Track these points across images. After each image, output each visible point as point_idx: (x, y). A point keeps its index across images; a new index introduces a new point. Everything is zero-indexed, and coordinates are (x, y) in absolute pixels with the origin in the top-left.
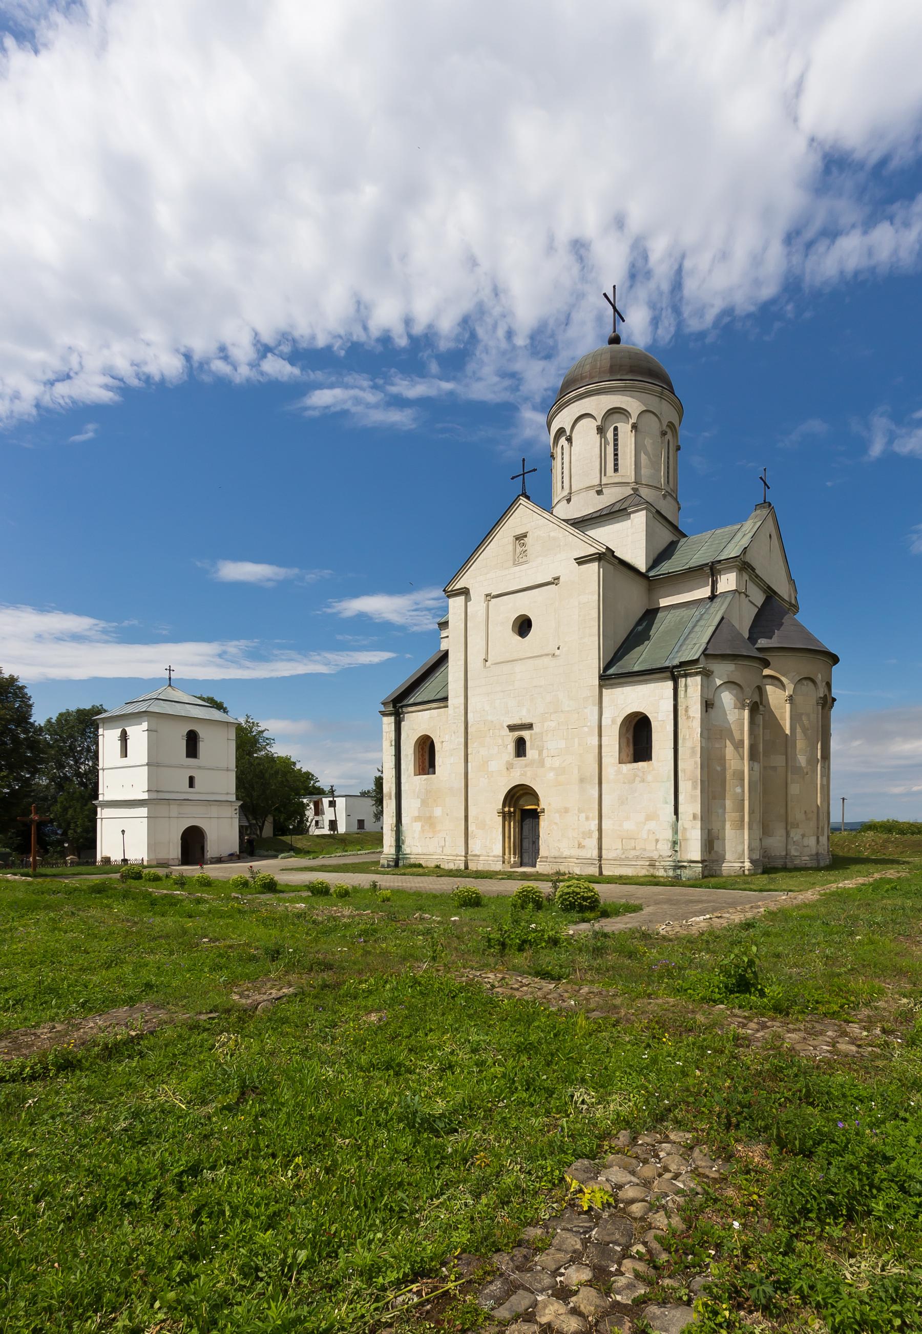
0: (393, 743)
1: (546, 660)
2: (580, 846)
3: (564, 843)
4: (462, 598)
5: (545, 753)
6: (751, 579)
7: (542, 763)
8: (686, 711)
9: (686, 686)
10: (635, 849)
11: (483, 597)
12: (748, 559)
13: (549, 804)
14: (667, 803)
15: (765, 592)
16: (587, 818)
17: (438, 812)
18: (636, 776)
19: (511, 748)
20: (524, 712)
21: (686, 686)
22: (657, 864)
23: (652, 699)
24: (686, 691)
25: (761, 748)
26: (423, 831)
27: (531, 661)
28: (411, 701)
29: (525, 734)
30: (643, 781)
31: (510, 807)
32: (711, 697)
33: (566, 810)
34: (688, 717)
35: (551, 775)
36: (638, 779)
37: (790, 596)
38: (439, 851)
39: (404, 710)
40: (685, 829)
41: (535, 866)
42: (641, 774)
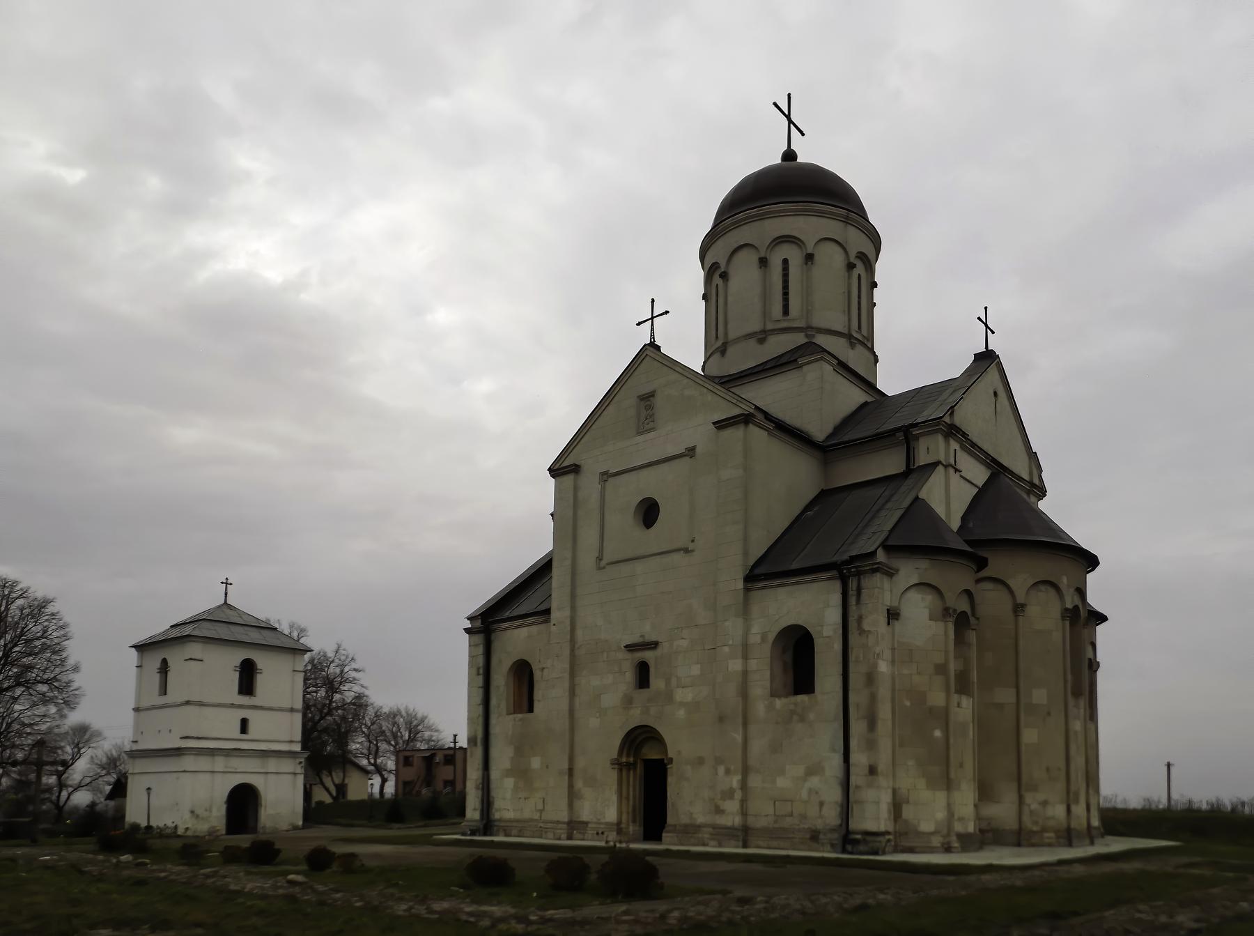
2: (719, 811)
5: (674, 681)
6: (963, 448)
7: (669, 697)
12: (957, 420)
13: (679, 752)
15: (988, 466)
16: (728, 772)
19: (630, 676)
20: (647, 628)
25: (974, 676)
28: (507, 614)
29: (648, 656)
30: (802, 719)
31: (628, 756)
32: (895, 604)
35: (681, 713)
36: (795, 718)
37: (1031, 474)
39: (496, 626)
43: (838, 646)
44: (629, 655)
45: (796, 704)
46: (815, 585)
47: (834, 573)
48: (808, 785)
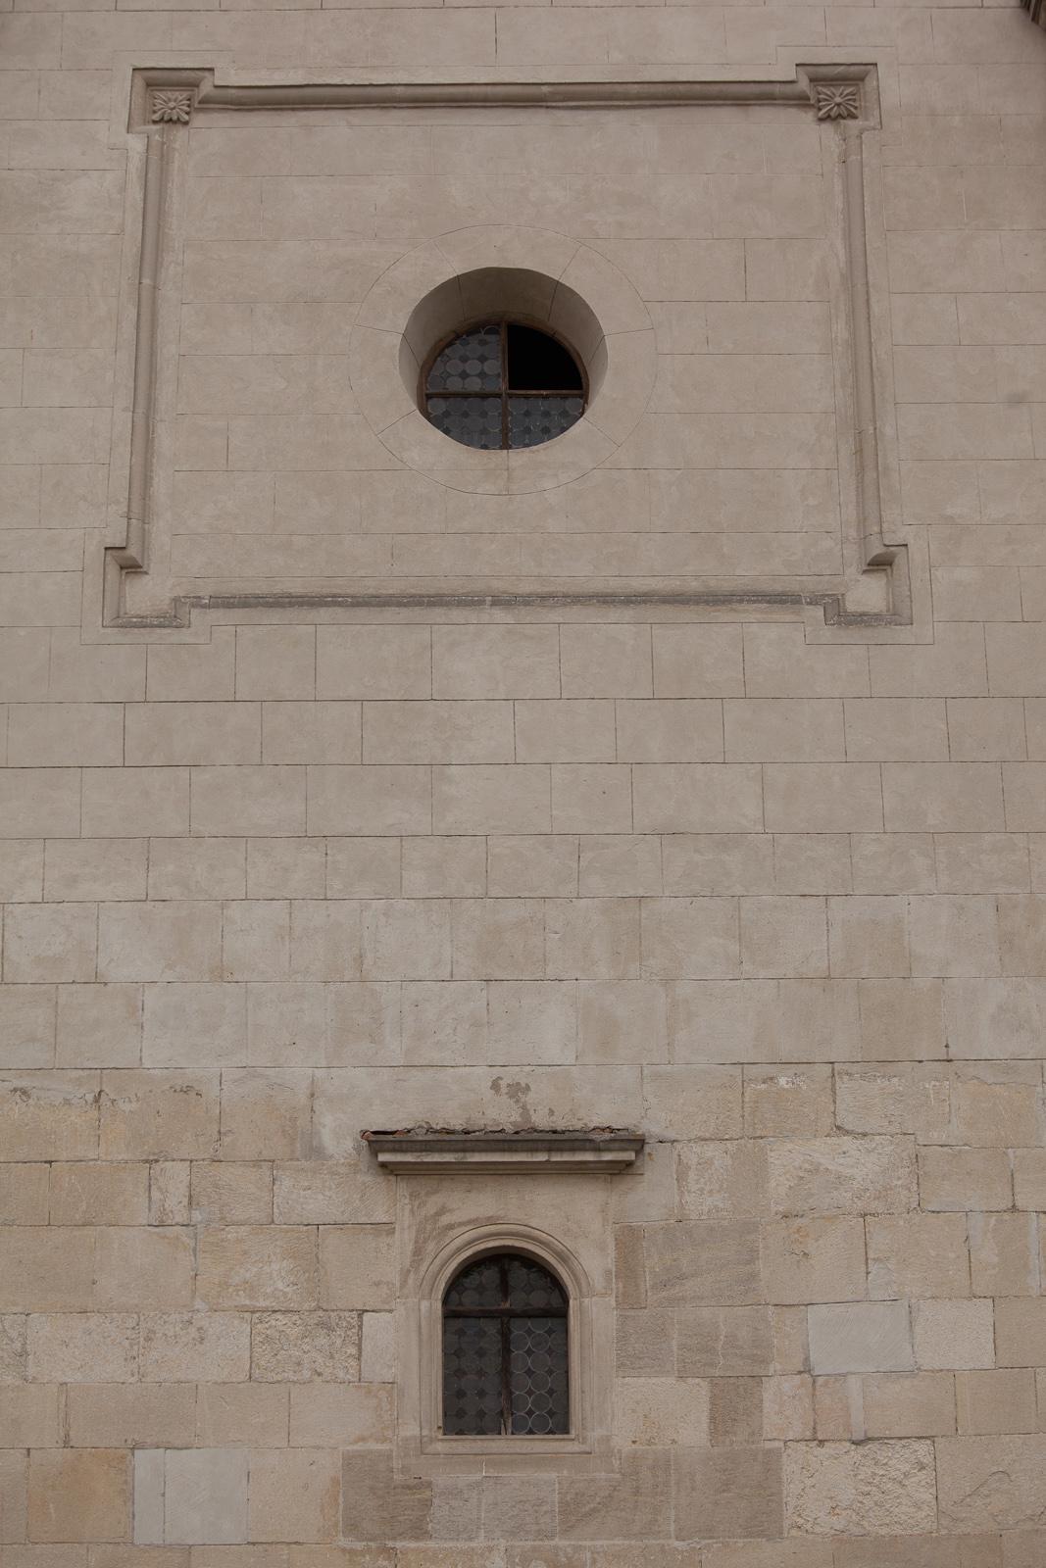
1: (771, 638)
5: (780, 1407)
11: (119, 94)
19: (404, 1341)
27: (619, 628)
44: (385, 1202)
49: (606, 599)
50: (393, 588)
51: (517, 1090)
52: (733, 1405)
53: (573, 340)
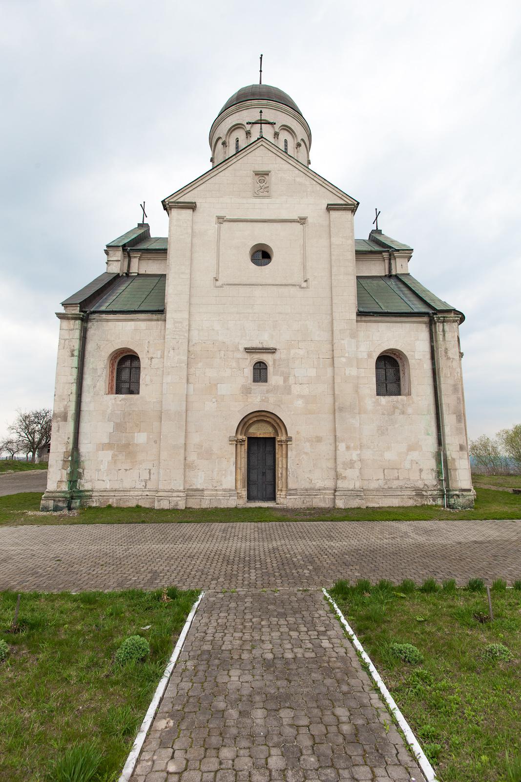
0: (76, 353)
1: (293, 290)
3: (304, 472)
4: (190, 211)
5: (291, 380)
7: (288, 390)
8: (446, 353)
9: (444, 331)
10: (398, 479)
11: (214, 219)
13: (298, 433)
14: (428, 434)
16: (348, 448)
17: (141, 438)
18: (395, 408)
19: (249, 372)
21: (444, 331)
22: (424, 493)
23: (409, 339)
24: (444, 335)
26: (115, 460)
30: (403, 413)
33: (319, 440)
34: (448, 358)
35: (300, 403)
38: (140, 485)
40: (454, 460)
41: (274, 498)
42: (401, 407)
43: (427, 365)
44: (247, 356)
45: (397, 402)
46: (408, 325)
47: (426, 319)
48: (409, 457)
49: (273, 285)
50: (248, 283)
51: (262, 343)
52: (286, 380)
53: (269, 253)
